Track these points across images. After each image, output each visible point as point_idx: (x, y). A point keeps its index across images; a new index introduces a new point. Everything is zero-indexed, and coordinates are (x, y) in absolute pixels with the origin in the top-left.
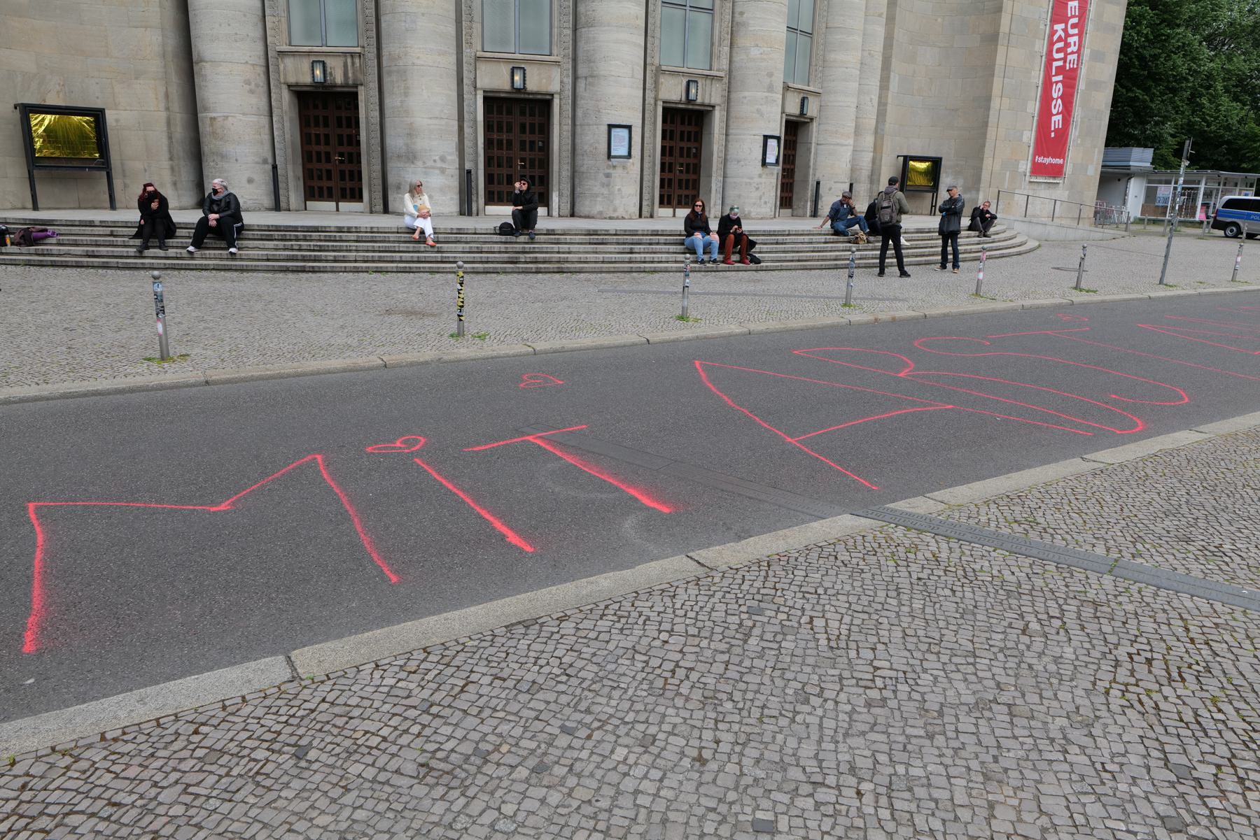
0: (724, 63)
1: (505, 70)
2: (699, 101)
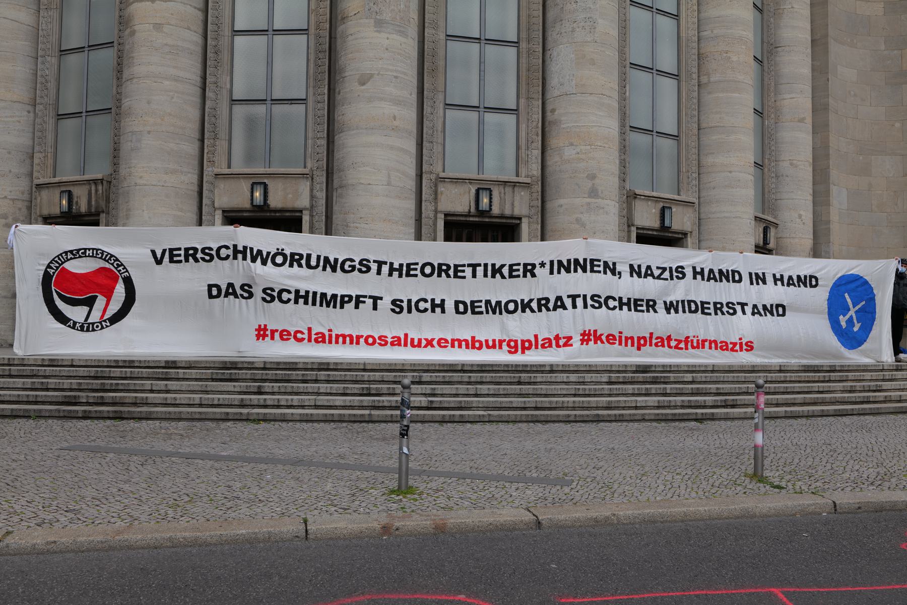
1: (245, 186)
2: (496, 210)
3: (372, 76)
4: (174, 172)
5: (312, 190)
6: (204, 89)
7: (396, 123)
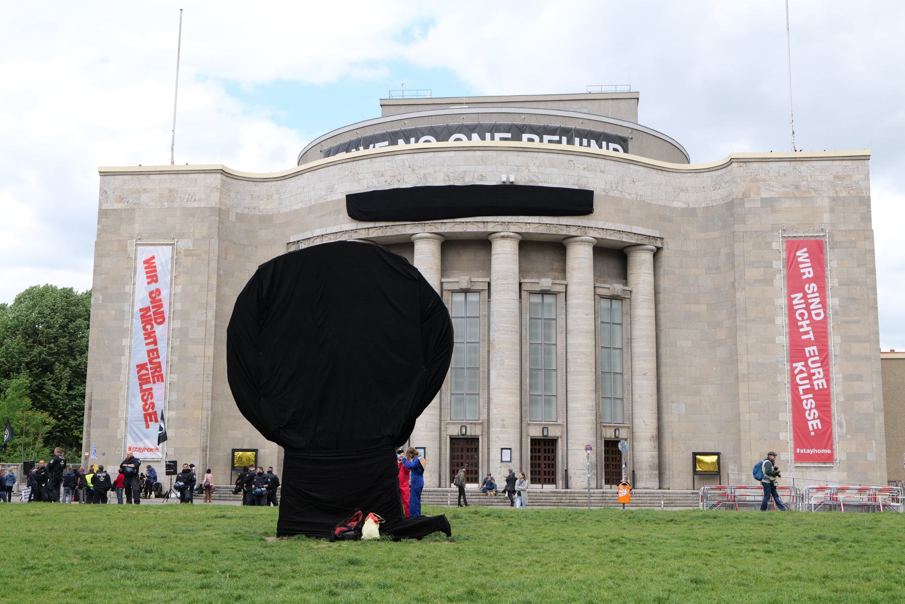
0: (485, 417)
2: (468, 433)
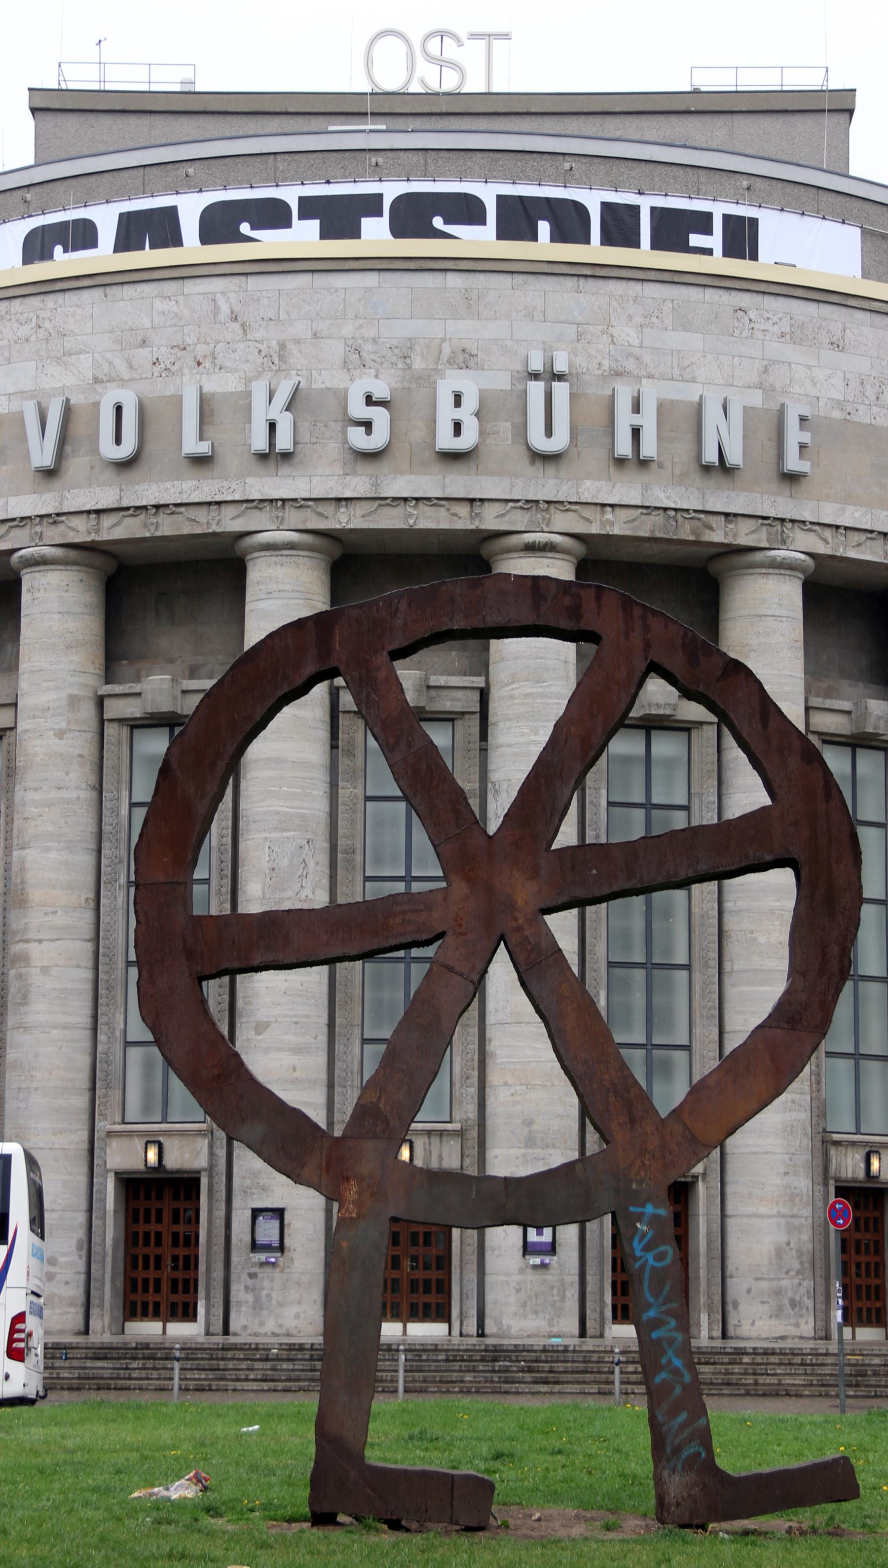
0: (470, 1111)
1: (139, 1144)
3: (267, 1025)
4: (62, 1131)
5: (211, 1147)
6: (95, 1029)
7: (295, 1075)
